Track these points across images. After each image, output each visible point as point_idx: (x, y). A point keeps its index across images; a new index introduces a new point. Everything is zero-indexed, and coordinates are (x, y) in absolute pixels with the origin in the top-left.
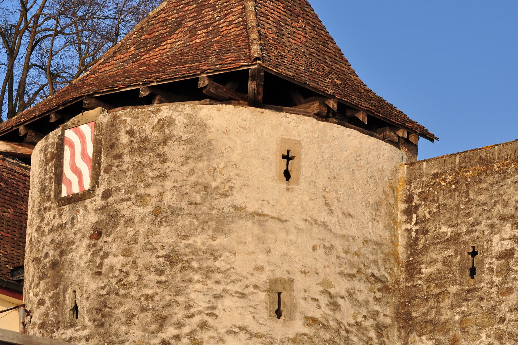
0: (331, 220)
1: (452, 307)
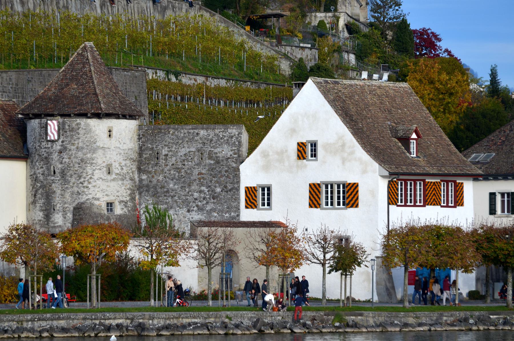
0: (120, 146)
1: (152, 167)
